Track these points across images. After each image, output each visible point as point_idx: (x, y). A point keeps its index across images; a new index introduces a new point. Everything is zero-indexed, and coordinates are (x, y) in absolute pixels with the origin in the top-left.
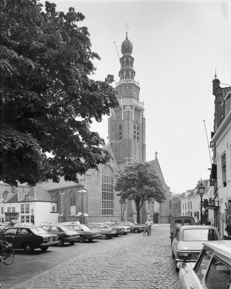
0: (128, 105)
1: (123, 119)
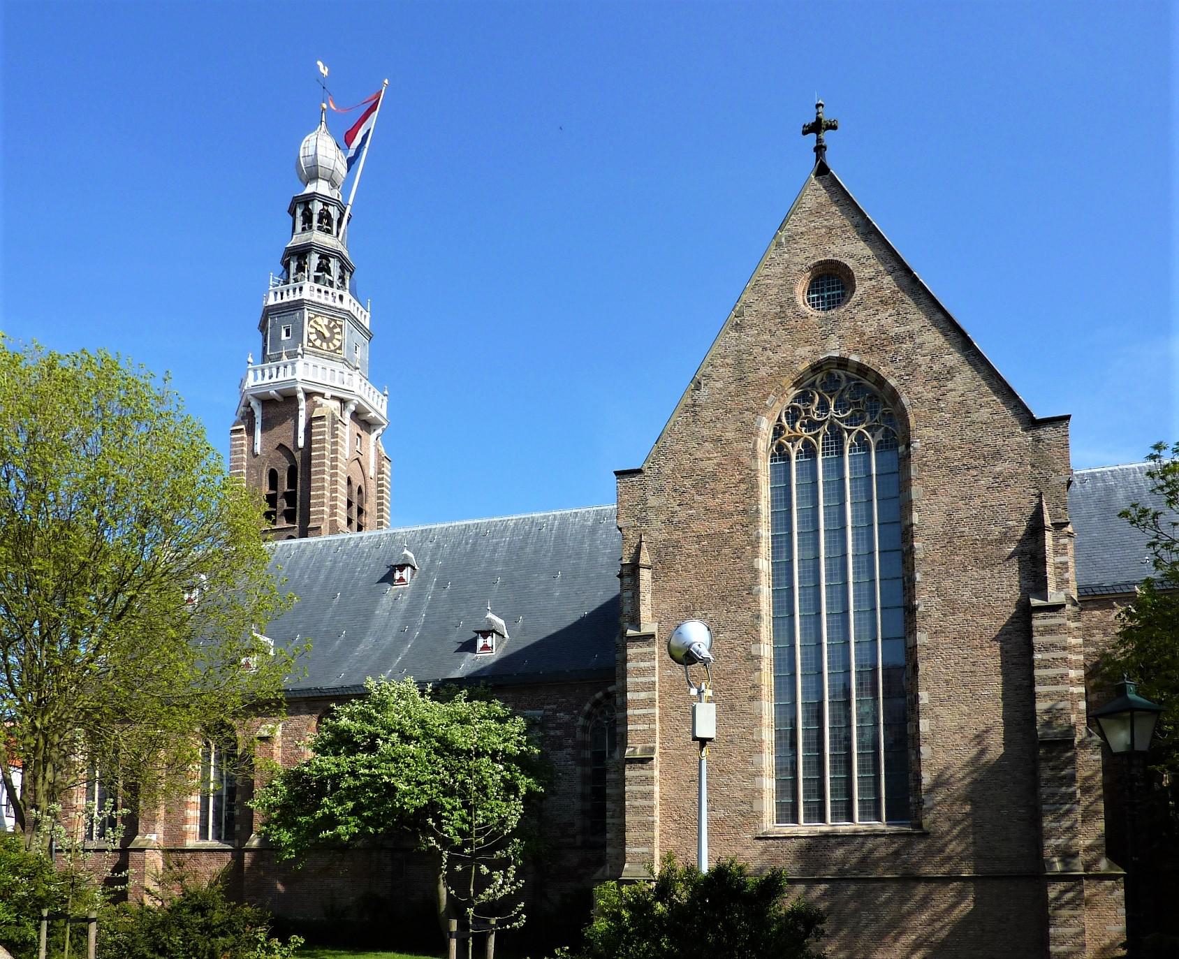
0: (328, 394)
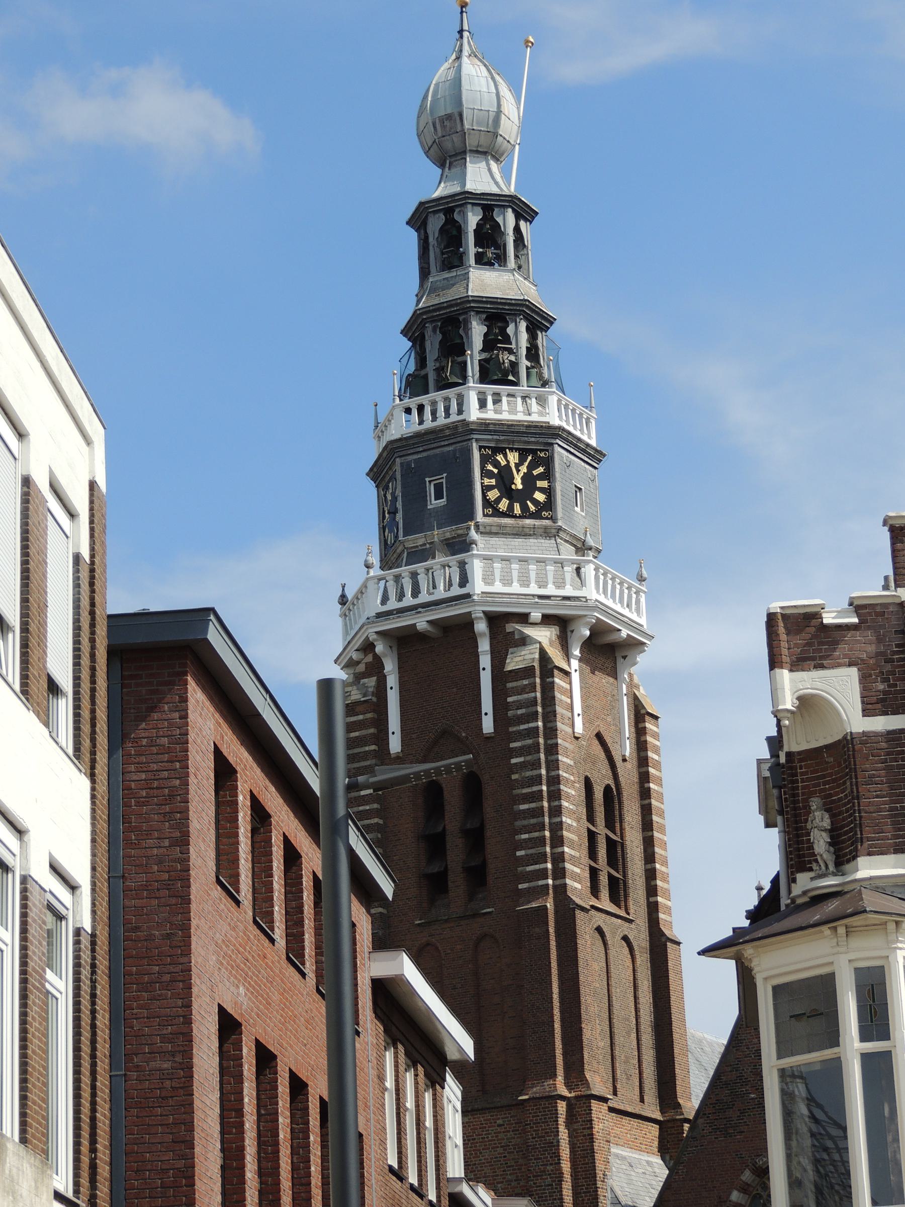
0: (536, 616)
1: (488, 725)
